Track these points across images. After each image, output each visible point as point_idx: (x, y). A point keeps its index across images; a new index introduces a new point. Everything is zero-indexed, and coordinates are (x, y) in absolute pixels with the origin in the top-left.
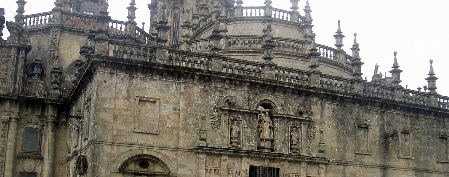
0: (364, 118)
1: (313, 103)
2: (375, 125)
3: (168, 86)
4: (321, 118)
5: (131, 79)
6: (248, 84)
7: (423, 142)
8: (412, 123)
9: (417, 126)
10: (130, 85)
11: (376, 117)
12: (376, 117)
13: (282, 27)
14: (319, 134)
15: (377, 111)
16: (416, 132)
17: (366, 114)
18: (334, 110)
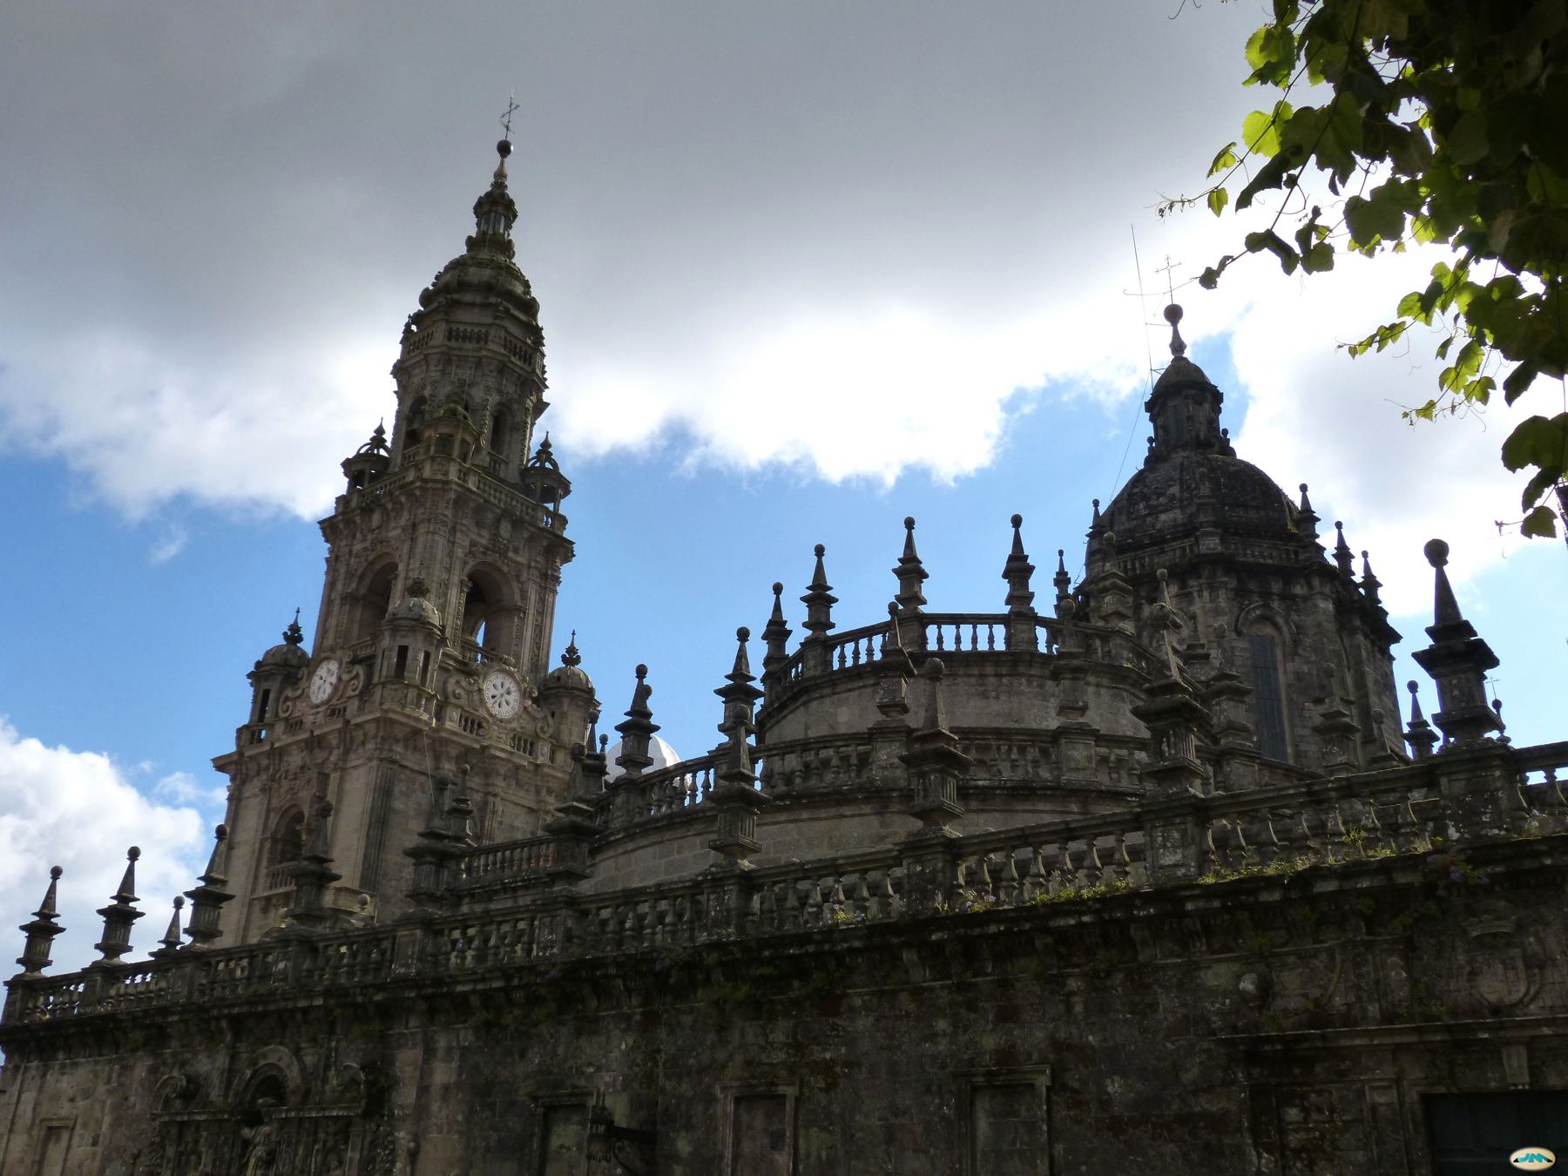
0: (571, 1062)
1: (402, 1041)
2: (614, 1086)
3: (96, 1075)
4: (419, 1097)
5: (44, 1075)
6: (224, 1024)
7: (860, 1135)
8: (799, 1037)
9: (824, 1050)
10: (40, 1090)
11: (623, 1047)
12: (623, 1047)
13: (857, 693)
14: (405, 1167)
15: (629, 1018)
16: (822, 1084)
17: (583, 1041)
18: (465, 1052)
